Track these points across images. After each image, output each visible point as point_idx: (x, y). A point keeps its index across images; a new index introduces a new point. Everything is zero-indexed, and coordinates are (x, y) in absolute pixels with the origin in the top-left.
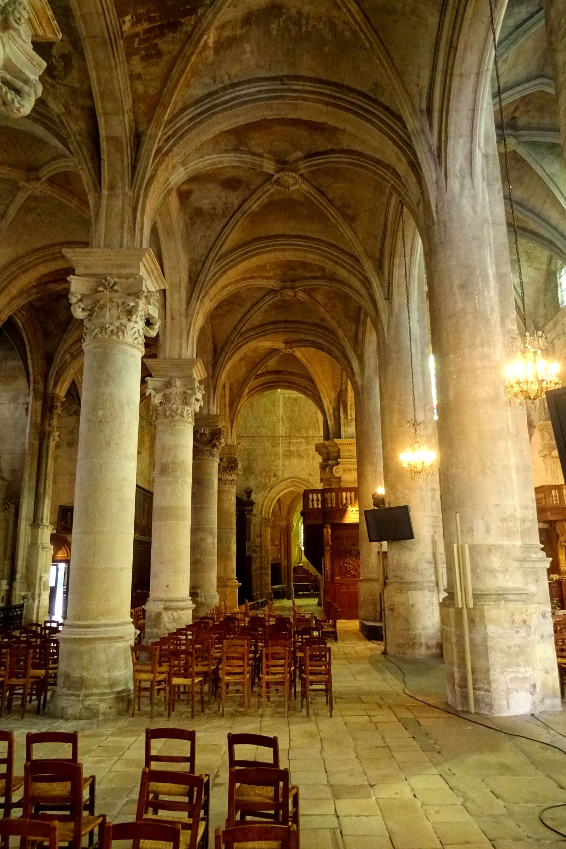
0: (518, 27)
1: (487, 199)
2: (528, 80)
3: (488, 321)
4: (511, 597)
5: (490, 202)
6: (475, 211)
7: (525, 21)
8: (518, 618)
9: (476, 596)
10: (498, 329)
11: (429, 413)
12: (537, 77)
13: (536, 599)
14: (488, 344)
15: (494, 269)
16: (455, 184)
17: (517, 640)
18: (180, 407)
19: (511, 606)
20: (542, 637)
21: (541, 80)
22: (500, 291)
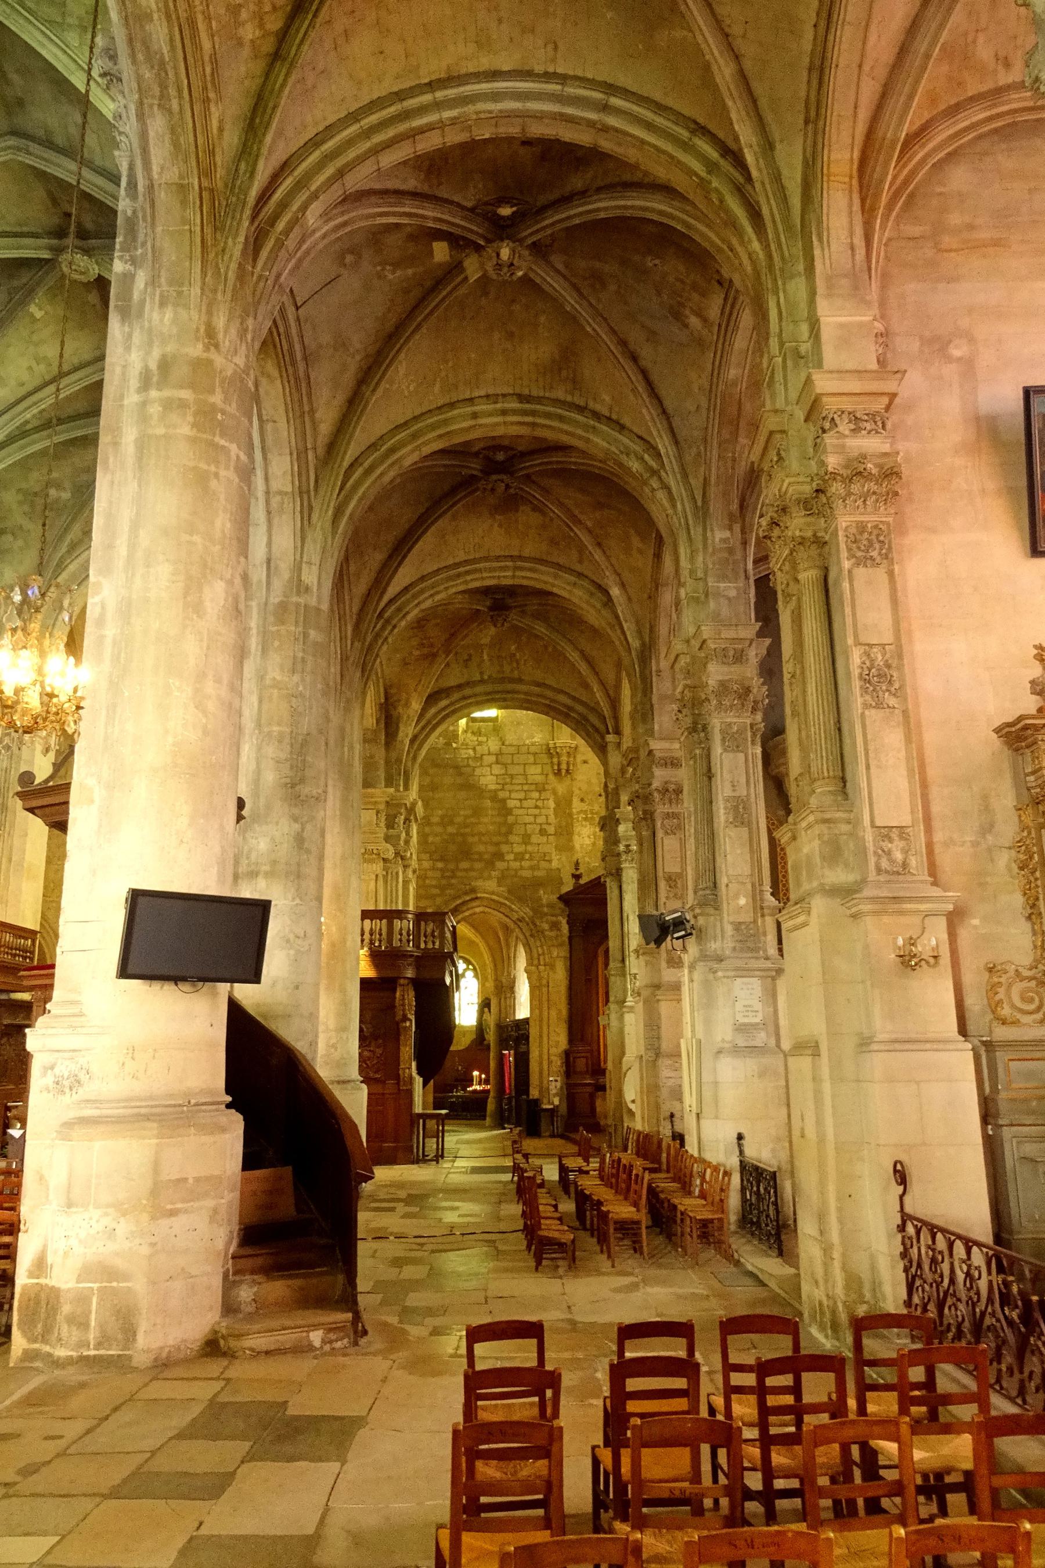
21: (12, 141)
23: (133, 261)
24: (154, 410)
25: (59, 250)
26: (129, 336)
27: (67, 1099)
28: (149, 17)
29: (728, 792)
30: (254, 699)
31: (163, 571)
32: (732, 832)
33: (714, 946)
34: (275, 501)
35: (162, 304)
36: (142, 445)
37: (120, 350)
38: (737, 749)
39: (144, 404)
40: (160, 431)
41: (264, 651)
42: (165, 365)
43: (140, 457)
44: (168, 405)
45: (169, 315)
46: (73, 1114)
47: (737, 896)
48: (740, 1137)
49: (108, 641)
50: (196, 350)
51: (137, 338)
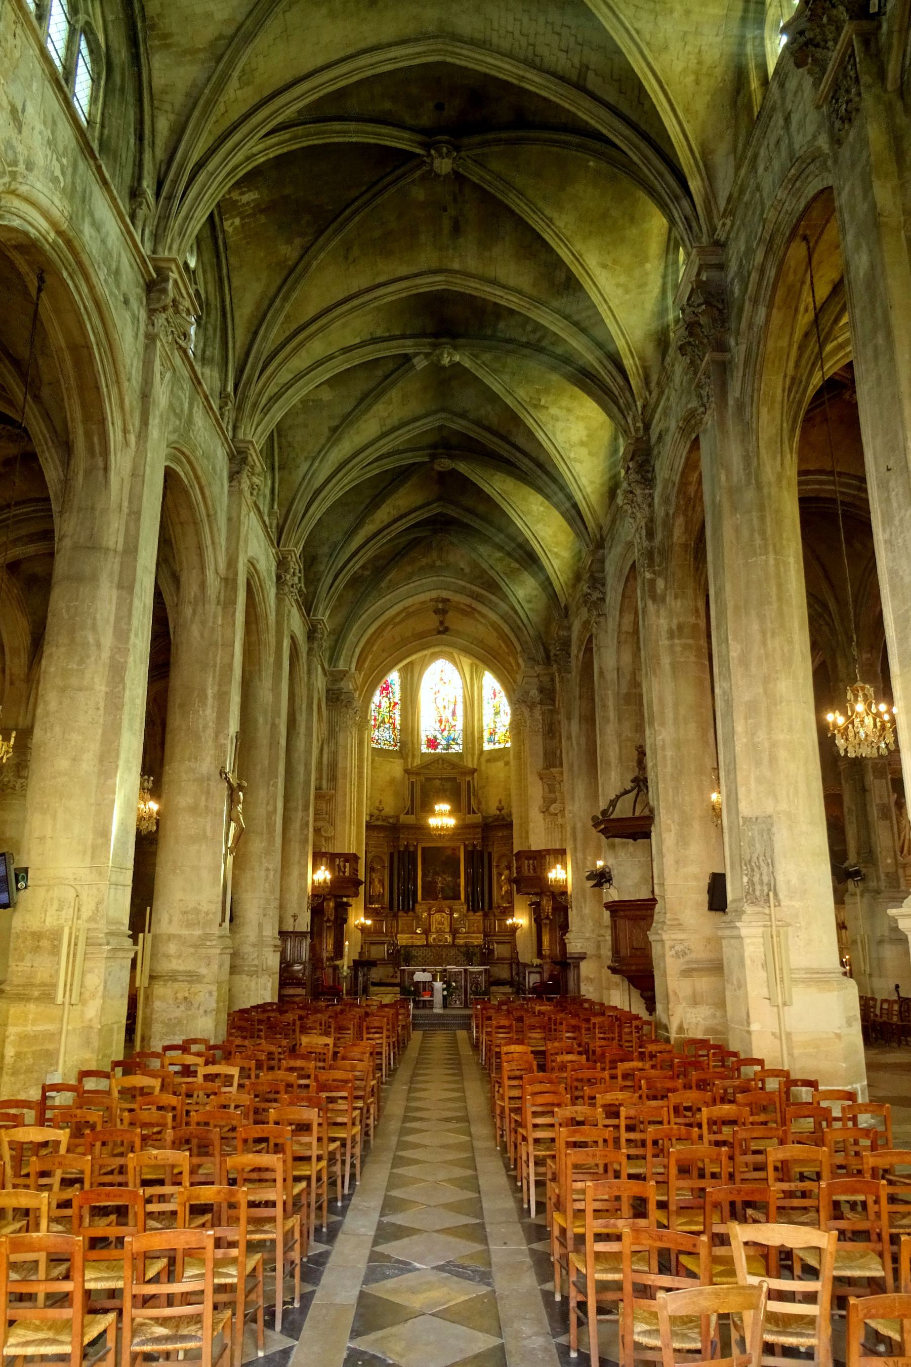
0: (386, 377)
1: (220, 622)
2: (426, 415)
3: (199, 738)
4: (181, 978)
5: (222, 625)
6: (202, 636)
7: (393, 372)
8: (180, 996)
9: (152, 978)
10: (210, 743)
11: (272, 788)
12: (436, 412)
13: (205, 980)
14: (196, 759)
15: (216, 688)
16: (188, 611)
17: (178, 1013)
18: (12, 779)
19: (176, 985)
20: (205, 1012)
21: (444, 415)
22: (219, 708)
23: (654, 572)
24: (678, 649)
25: (433, 457)
26: (658, 611)
27: (682, 960)
28: (691, 483)
29: (878, 801)
30: (616, 747)
31: (692, 726)
32: (882, 823)
33: (873, 884)
34: (623, 636)
35: (676, 598)
36: (674, 665)
37: (654, 618)
38: (881, 778)
39: (672, 646)
40: (682, 660)
41: (620, 720)
42: (680, 627)
43: (674, 672)
44: (685, 647)
45: (679, 603)
46: (684, 967)
47: (886, 858)
48: (897, 987)
49: (668, 757)
50: (692, 620)
51: (663, 612)
